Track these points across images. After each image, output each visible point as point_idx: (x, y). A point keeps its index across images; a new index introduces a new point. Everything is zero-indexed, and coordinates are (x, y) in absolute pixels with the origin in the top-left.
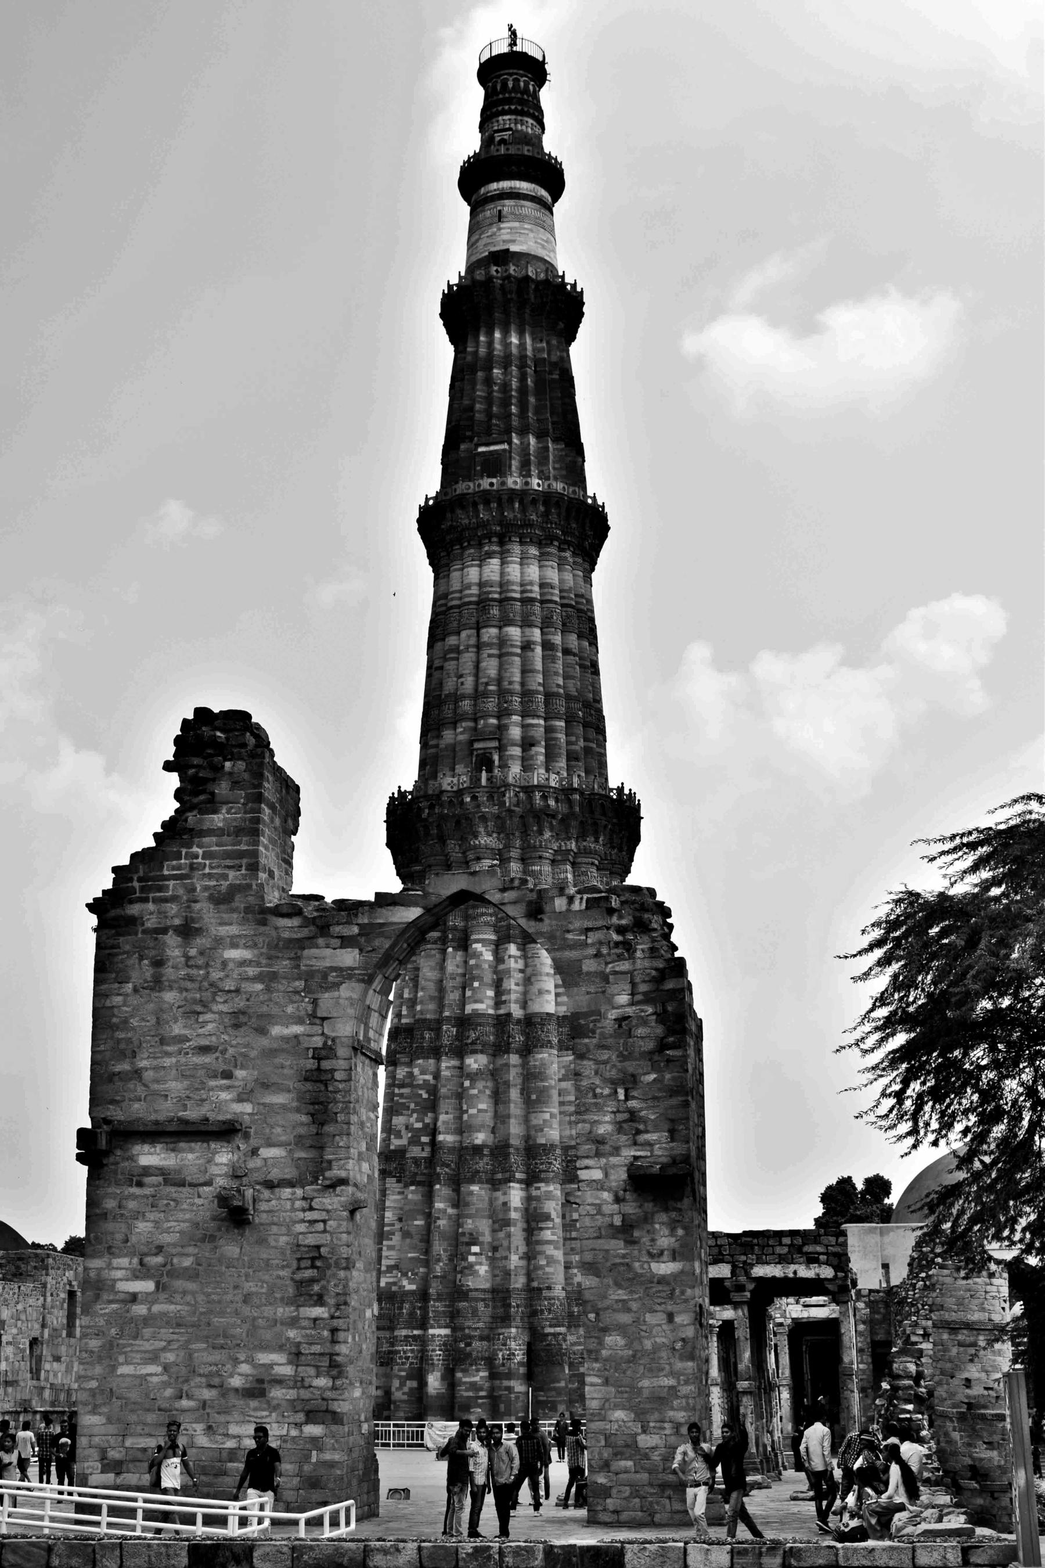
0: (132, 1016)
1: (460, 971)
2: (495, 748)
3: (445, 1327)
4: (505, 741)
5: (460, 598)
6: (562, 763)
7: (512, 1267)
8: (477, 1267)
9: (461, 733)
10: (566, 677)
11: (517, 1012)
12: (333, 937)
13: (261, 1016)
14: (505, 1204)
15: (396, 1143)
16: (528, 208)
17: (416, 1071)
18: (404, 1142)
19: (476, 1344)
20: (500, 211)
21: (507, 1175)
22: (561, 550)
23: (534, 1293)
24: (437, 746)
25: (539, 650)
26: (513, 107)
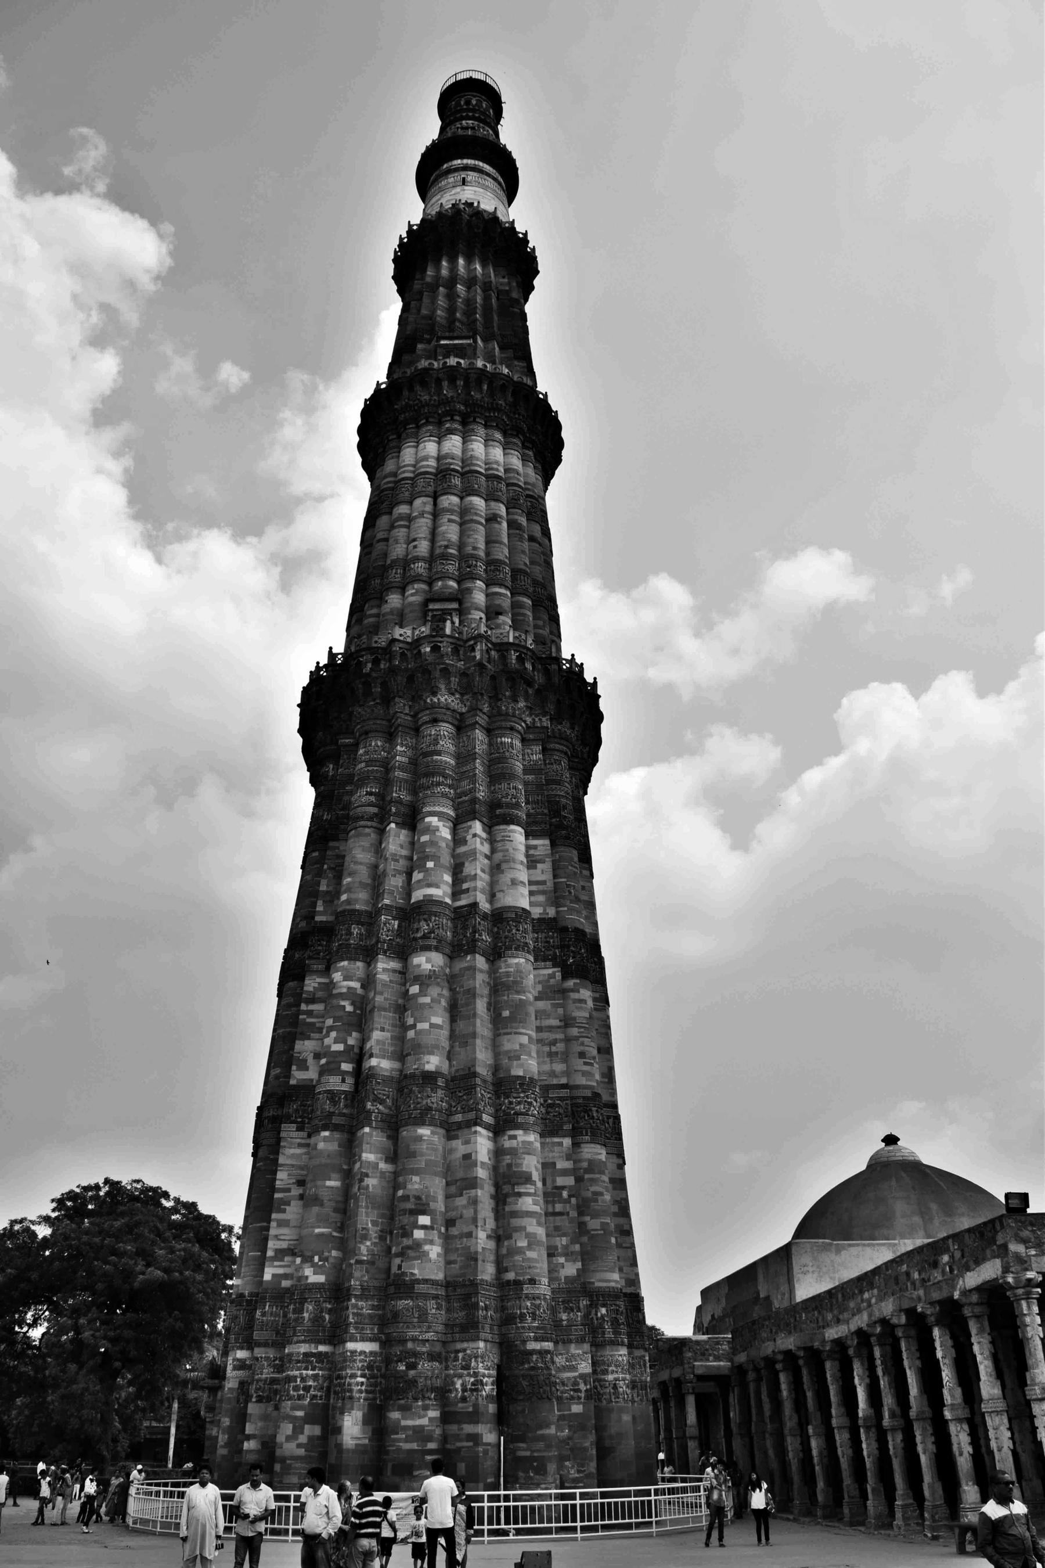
2: (455, 610)
3: (371, 1340)
5: (414, 472)
7: (480, 1250)
8: (427, 1247)
9: (412, 595)
10: (532, 563)
11: (485, 906)
14: (467, 1157)
15: (298, 1076)
16: (489, 182)
17: (337, 976)
18: (312, 1074)
19: (425, 1366)
20: (464, 179)
21: (472, 1115)
22: (524, 447)
23: (509, 1289)
25: (505, 525)
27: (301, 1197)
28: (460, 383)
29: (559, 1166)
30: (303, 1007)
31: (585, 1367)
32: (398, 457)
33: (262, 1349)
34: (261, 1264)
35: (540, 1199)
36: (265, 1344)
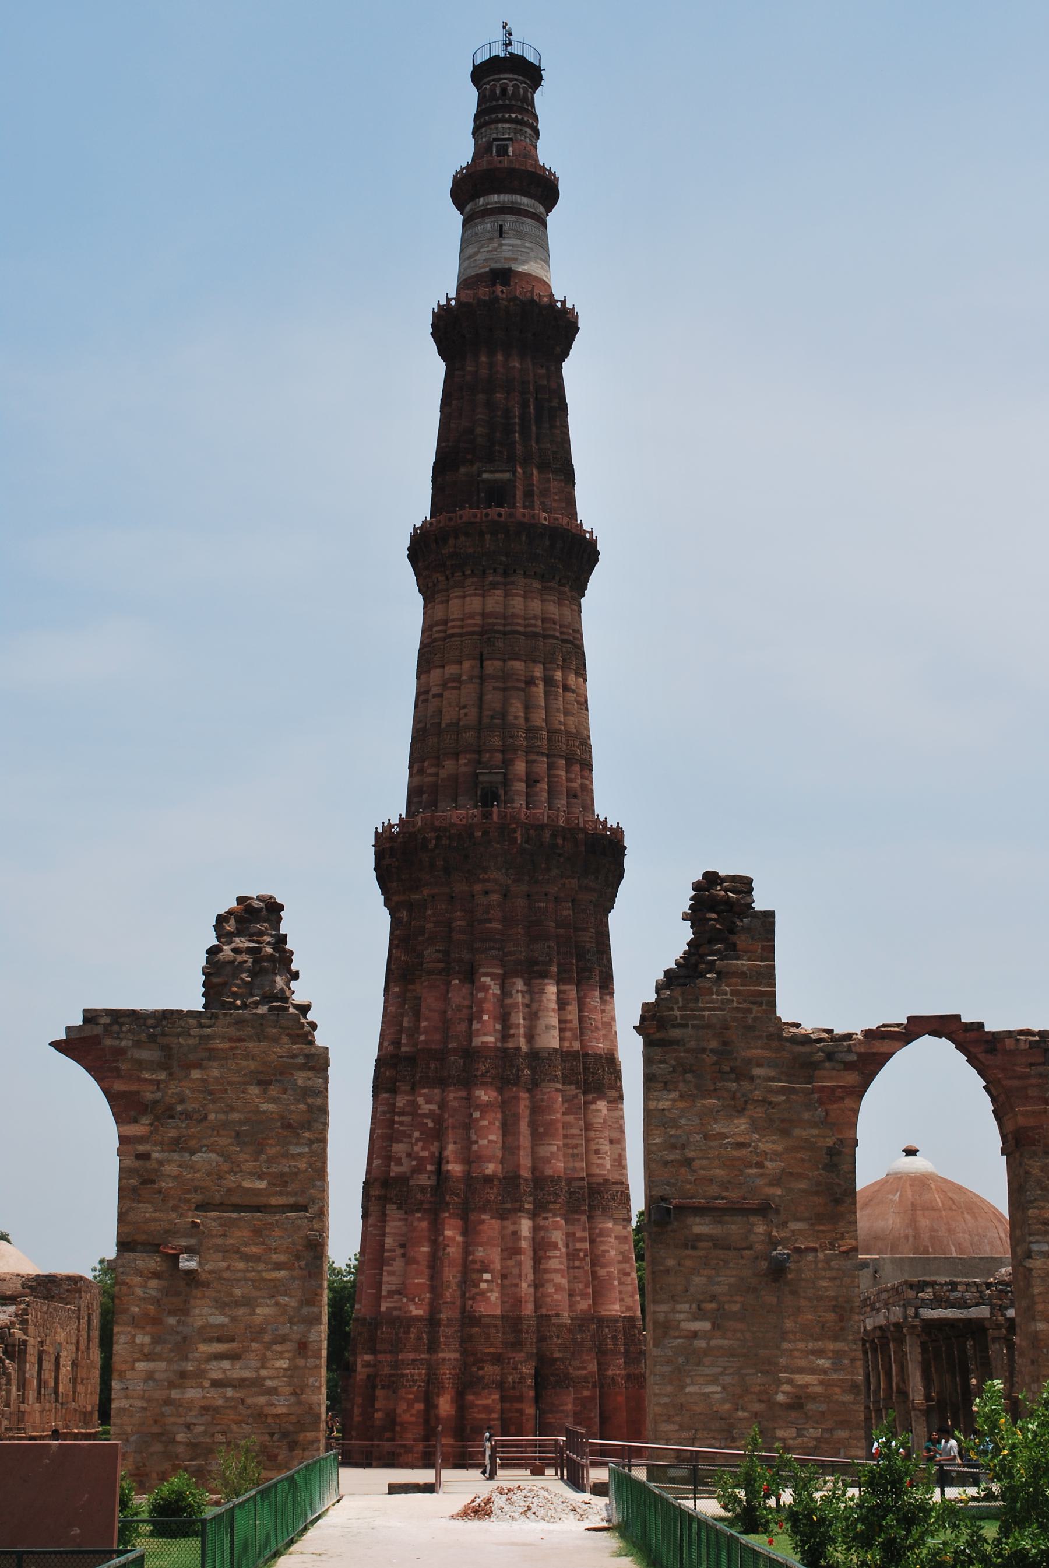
0: (680, 1117)
1: (466, 1003)
3: (456, 1351)
4: (510, 777)
5: (462, 627)
6: (564, 802)
12: (837, 1062)
13: (783, 1121)
15: (395, 1170)
17: (421, 1100)
20: (501, 226)
23: (543, 1319)
24: (437, 775)
26: (514, 116)
27: (403, 1255)
28: (501, 536)
29: (579, 1234)
30: (397, 1118)
31: (593, 1367)
32: (448, 601)
33: (383, 1355)
34: (378, 1298)
35: (564, 1260)
36: (385, 1352)
